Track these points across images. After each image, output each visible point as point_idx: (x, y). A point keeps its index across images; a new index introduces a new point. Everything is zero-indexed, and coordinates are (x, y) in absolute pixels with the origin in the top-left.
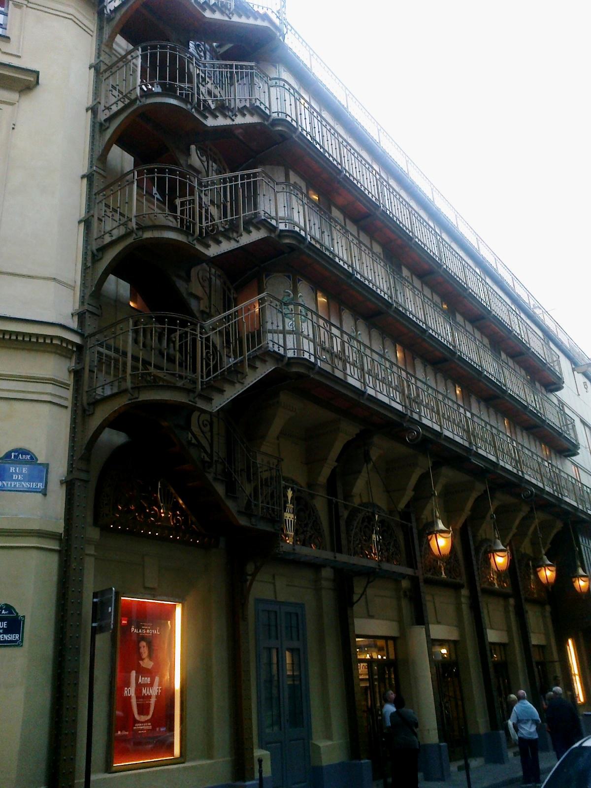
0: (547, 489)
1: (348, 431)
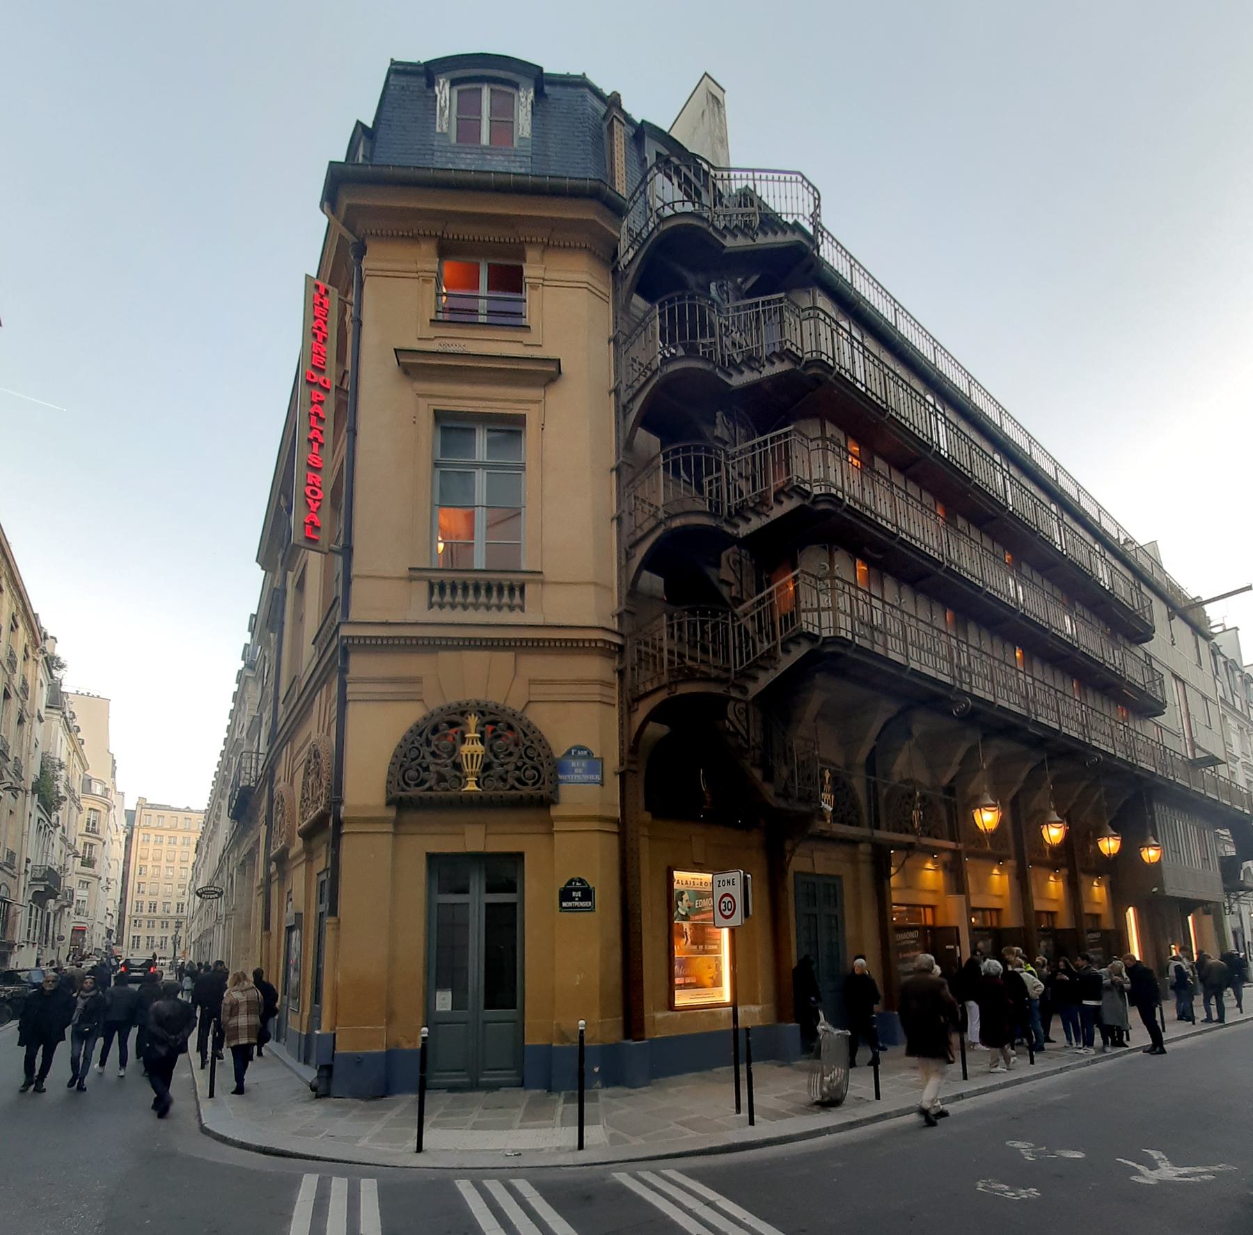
0: (1119, 754)
1: (887, 708)
